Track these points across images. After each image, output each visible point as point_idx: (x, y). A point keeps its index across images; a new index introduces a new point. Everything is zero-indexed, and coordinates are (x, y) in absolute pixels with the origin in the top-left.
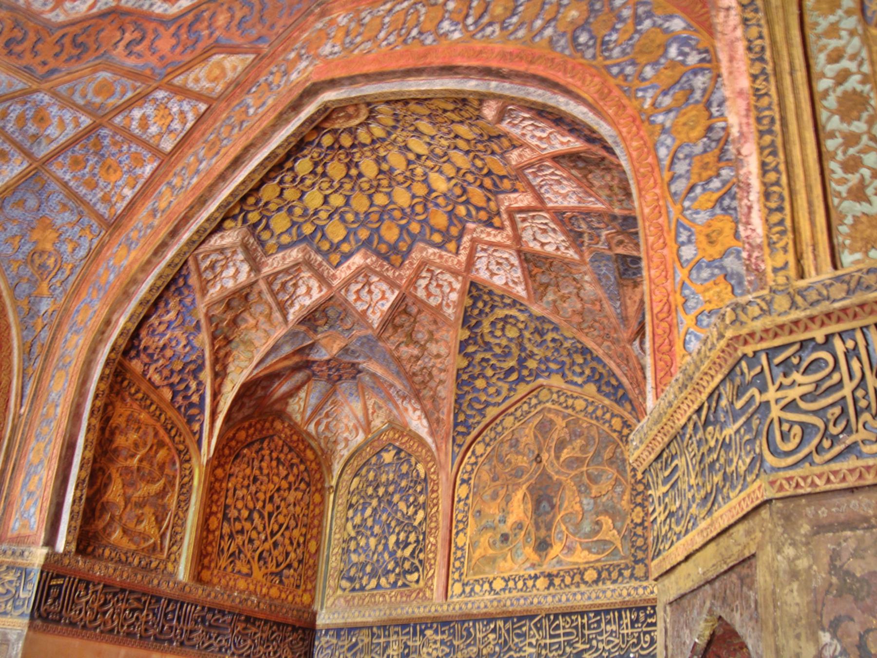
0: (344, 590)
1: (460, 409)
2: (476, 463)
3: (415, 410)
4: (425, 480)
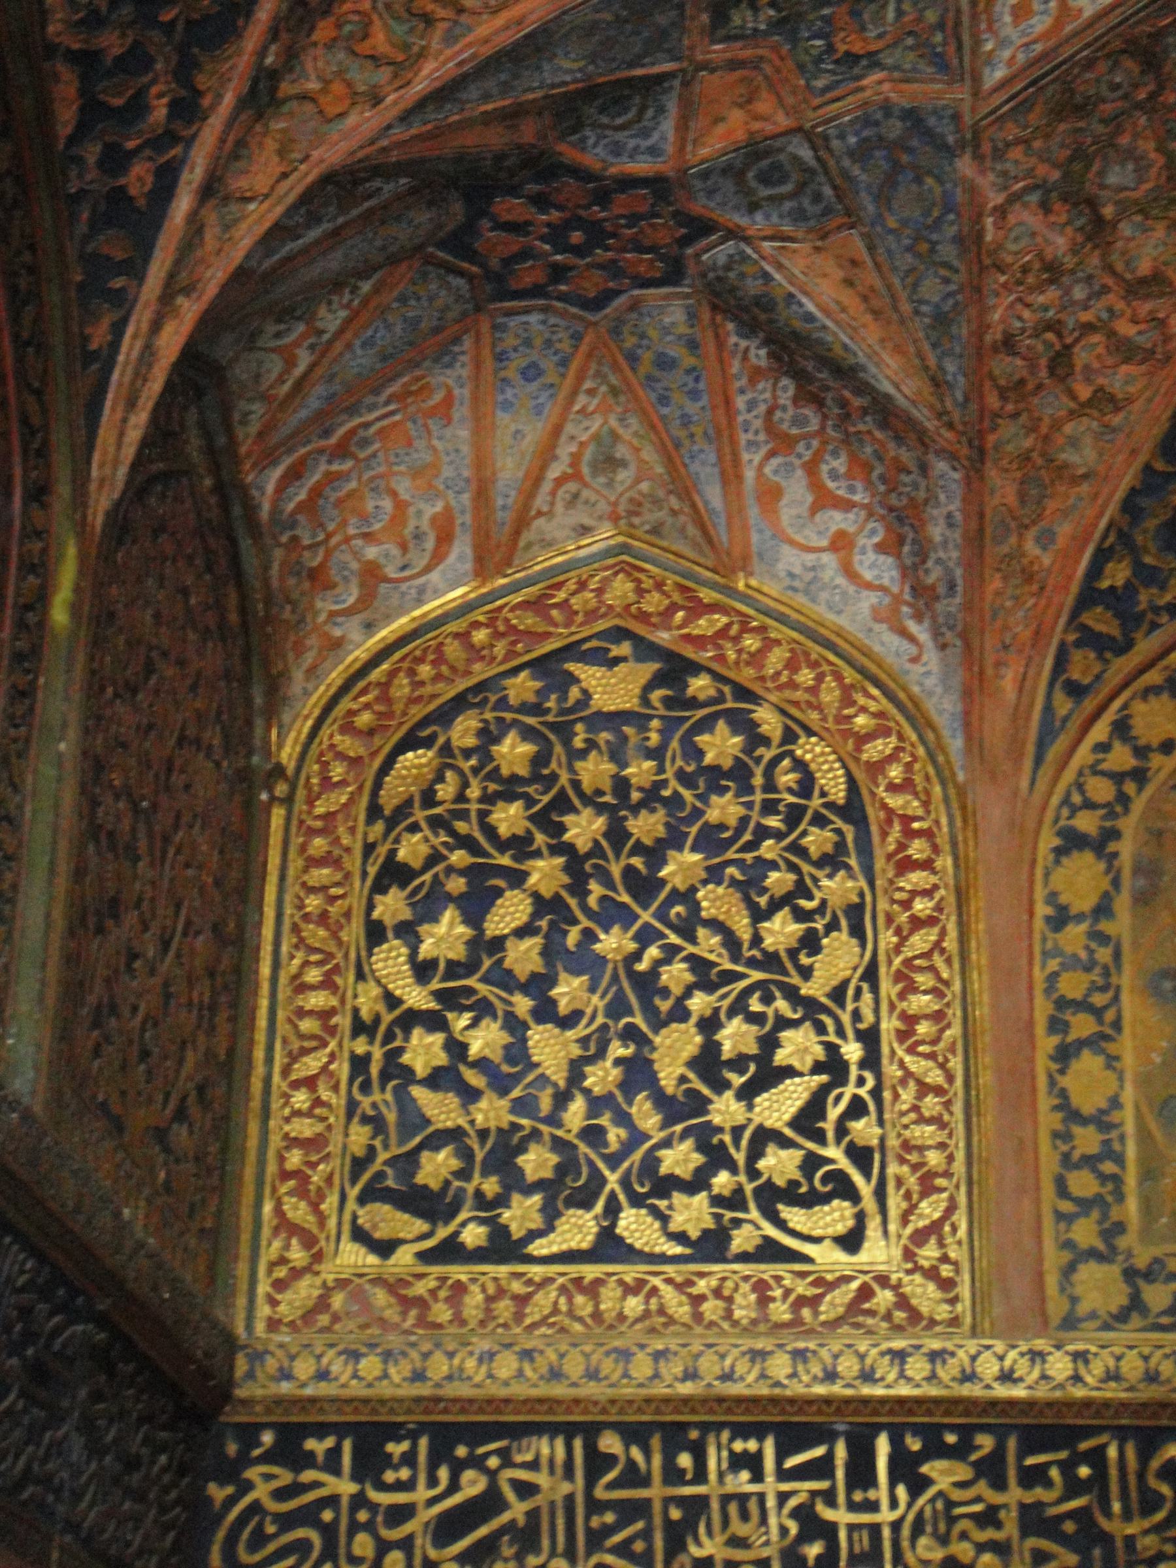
0: (385, 1248)
1: (1124, 538)
2: (1140, 776)
3: (823, 500)
4: (852, 809)
